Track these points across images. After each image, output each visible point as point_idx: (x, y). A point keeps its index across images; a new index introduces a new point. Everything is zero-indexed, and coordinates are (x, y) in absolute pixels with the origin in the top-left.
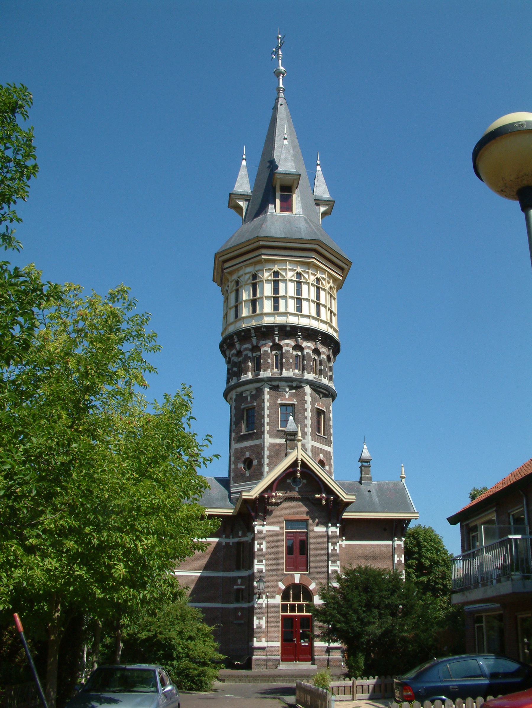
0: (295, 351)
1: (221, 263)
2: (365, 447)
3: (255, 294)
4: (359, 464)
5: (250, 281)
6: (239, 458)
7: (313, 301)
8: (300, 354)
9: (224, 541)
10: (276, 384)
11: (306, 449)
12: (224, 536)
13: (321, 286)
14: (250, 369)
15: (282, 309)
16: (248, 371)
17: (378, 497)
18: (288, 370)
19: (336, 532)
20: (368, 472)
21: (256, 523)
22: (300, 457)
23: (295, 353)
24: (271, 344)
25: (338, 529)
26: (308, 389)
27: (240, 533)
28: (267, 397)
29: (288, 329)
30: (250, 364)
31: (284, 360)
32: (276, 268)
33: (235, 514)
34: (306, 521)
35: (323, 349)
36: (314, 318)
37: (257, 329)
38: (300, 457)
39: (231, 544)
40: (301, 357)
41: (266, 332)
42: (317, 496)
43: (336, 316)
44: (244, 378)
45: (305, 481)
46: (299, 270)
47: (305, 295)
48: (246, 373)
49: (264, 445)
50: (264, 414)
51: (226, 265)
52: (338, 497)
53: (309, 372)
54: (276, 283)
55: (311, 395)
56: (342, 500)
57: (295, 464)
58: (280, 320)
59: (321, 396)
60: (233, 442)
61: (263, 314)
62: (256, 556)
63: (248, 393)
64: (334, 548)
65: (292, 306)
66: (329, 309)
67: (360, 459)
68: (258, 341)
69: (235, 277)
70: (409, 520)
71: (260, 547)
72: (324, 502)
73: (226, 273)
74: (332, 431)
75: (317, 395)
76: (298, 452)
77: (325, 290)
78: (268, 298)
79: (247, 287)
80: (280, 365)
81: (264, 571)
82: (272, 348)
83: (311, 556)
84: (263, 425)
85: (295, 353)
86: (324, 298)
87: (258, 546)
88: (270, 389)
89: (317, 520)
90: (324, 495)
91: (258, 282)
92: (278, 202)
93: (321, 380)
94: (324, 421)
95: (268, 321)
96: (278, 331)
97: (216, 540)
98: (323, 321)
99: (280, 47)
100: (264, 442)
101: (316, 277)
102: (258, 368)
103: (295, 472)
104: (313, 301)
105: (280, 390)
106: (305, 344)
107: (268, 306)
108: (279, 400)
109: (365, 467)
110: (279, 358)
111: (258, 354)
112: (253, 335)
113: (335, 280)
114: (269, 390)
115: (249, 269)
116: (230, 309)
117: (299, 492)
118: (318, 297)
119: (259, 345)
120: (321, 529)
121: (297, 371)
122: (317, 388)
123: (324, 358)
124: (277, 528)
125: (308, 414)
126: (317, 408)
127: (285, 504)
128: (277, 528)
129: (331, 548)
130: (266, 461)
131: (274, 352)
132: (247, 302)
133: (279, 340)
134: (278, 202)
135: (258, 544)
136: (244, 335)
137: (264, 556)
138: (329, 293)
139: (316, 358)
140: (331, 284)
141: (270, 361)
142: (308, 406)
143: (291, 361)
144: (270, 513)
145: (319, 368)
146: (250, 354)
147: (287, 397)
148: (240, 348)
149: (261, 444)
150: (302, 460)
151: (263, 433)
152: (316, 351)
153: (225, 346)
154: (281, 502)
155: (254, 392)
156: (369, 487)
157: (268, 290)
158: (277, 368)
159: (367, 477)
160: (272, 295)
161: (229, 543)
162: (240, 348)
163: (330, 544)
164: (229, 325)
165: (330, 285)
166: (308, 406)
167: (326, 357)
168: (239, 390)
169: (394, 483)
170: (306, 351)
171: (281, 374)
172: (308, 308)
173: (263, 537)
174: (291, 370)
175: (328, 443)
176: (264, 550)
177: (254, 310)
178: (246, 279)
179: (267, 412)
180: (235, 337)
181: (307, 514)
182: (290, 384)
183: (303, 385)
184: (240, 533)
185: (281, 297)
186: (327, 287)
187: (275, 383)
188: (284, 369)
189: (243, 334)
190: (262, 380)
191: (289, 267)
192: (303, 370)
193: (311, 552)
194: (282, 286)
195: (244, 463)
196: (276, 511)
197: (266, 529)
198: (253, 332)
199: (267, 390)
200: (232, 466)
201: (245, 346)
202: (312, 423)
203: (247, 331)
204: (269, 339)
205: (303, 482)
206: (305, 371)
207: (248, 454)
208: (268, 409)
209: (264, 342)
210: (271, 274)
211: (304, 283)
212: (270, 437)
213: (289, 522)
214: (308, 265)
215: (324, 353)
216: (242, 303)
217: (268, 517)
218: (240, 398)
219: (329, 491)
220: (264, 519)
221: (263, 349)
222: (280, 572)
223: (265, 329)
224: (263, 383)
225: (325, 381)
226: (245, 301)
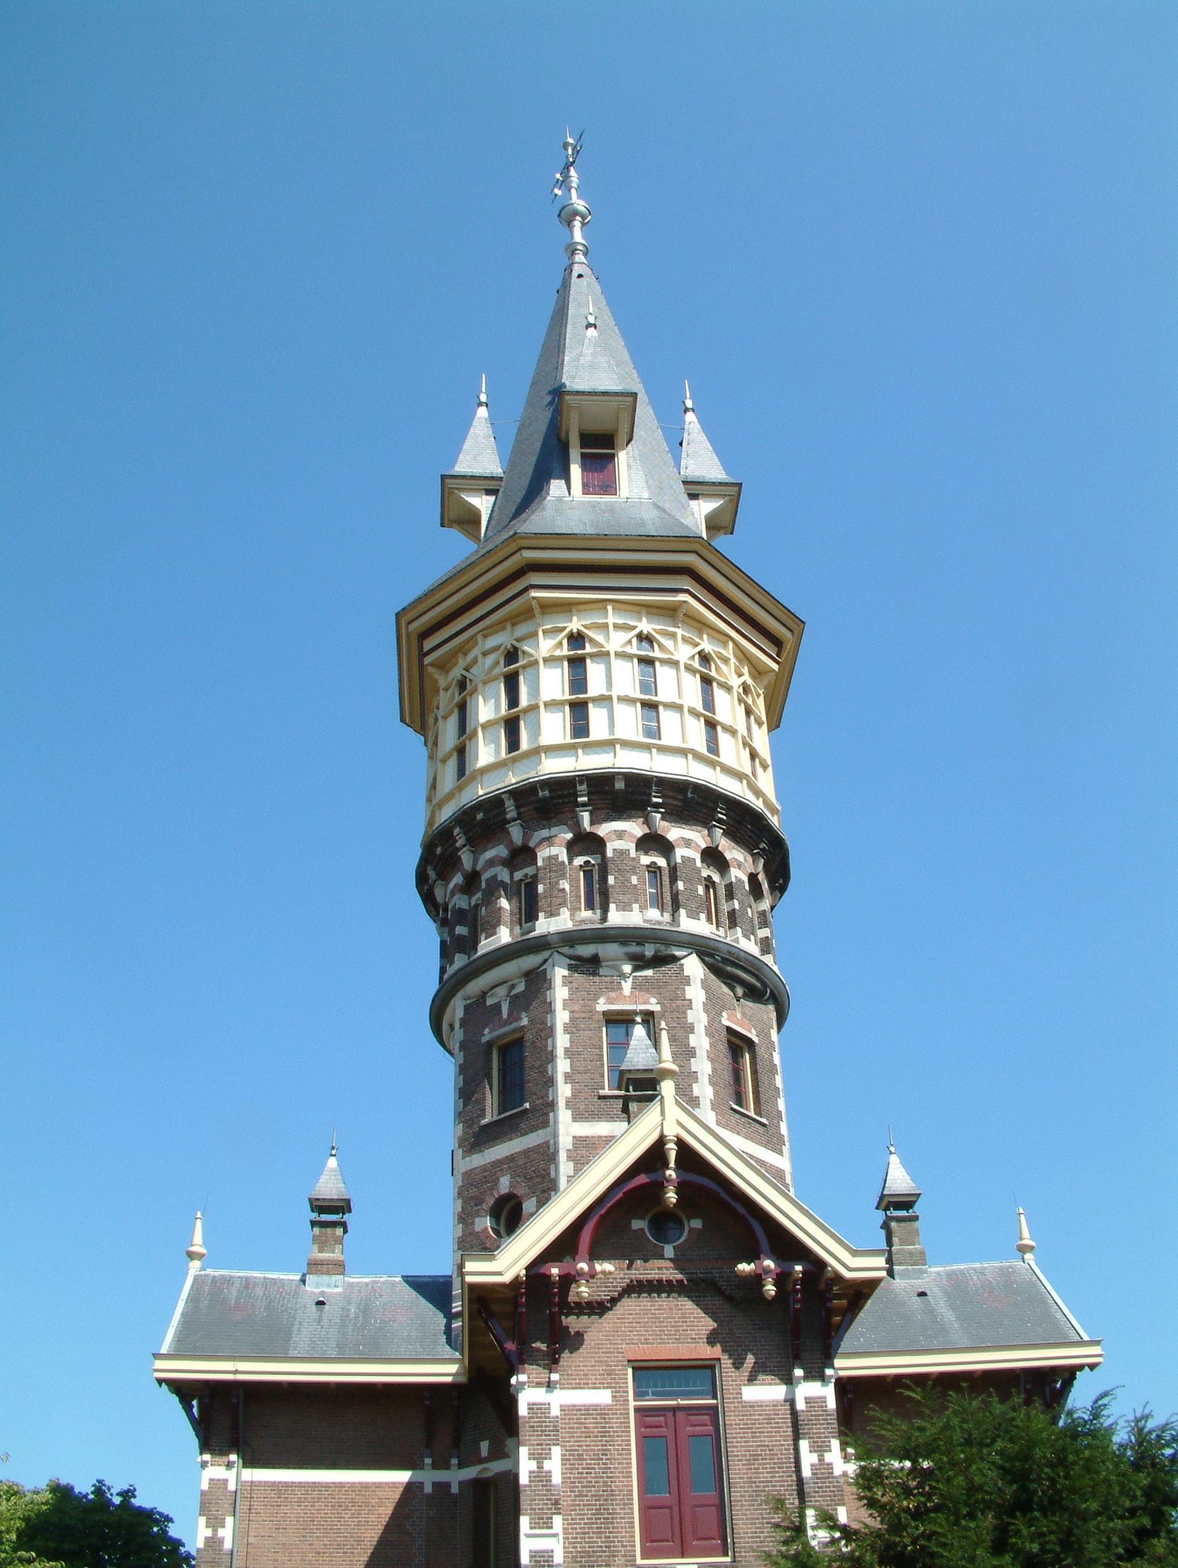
0: (646, 853)
1: (415, 643)
2: (894, 1160)
3: (513, 700)
4: (880, 1216)
5: (502, 669)
6: (479, 1201)
7: (693, 712)
8: (662, 862)
9: (429, 1477)
10: (587, 954)
11: (695, 1102)
12: (428, 1461)
13: (713, 673)
14: (506, 917)
16: (498, 923)
17: (953, 1307)
18: (625, 907)
19: (823, 1399)
20: (911, 1238)
21: (523, 1378)
23: (646, 860)
24: (569, 836)
25: (831, 1387)
26: (693, 966)
27: (484, 1447)
28: (560, 993)
29: (620, 785)
30: (504, 903)
31: (611, 880)
33: (463, 1379)
34: (709, 1367)
35: (733, 852)
36: (697, 756)
37: (524, 794)
38: (671, 1131)
39: (455, 1489)
40: (666, 873)
41: (550, 801)
42: (744, 1267)
43: (770, 770)
44: (486, 945)
45: (697, 1224)
46: (645, 626)
48: (492, 931)
49: (556, 1144)
50: (554, 1046)
51: (428, 644)
52: (821, 1264)
53: (693, 915)
54: (577, 664)
55: (705, 984)
56: (838, 1278)
57: (654, 1157)
59: (740, 991)
61: (537, 752)
62: (524, 1504)
63: (502, 991)
64: (821, 1459)
65: (629, 722)
66: (745, 744)
67: (882, 1197)
68: (528, 829)
69: (456, 672)
70: (1068, 1374)
71: (540, 1467)
72: (770, 1289)
73: (432, 664)
74: (777, 1059)
75: (725, 989)
76: (663, 1113)
77: (729, 689)
78: (552, 705)
79: (491, 687)
80: (599, 894)
81: (558, 1558)
83: (736, 1496)
84: (551, 1082)
86: (727, 709)
87: (533, 1465)
88: (571, 968)
89: (750, 1360)
90: (769, 1263)
91: (524, 667)
92: (576, 471)
93: (737, 940)
94: (755, 1072)
95: (554, 767)
96: (589, 794)
97: (403, 1476)
99: (572, 164)
100: (555, 1135)
101: (698, 649)
103: (659, 1187)
104: (693, 712)
105: (602, 971)
106: (674, 833)
107: (554, 727)
108: (602, 1000)
109: (900, 1220)
110: (596, 877)
111: (530, 871)
112: (511, 813)
113: (758, 672)
114: (566, 972)
116: (444, 761)
117: (677, 1262)
118: (709, 703)
119: (531, 844)
120: (769, 1392)
122: (724, 965)
123: (739, 880)
124: (602, 1397)
125: (700, 1041)
126: (729, 1030)
127: (629, 1305)
128: (602, 1397)
129: (808, 1459)
131: (579, 861)
132: (491, 730)
133: (592, 823)
134: (576, 471)
135: (532, 1456)
136: (484, 821)
137: (556, 1502)
138: (740, 700)
139: (716, 878)
140: (747, 678)
141: (567, 887)
142: (698, 1016)
143: (634, 880)
144: (575, 1341)
145: (725, 907)
146: (504, 875)
147: (628, 991)
148: (475, 862)
149: (547, 1143)
150: (680, 1142)
151: (552, 1106)
152: (713, 856)
153: (432, 874)
154: (614, 1301)
155: (521, 988)
156: (920, 1284)
157: (553, 683)
158: (590, 905)
159: (911, 1253)
160: (567, 696)
161: (447, 1485)
162: (475, 862)
163: (804, 1445)
164: (440, 805)
165: (742, 679)
166: (698, 1016)
167: (746, 879)
168: (474, 987)
169: (1001, 1268)
170: (680, 853)
171: (604, 919)
173: (550, 1429)
174: (636, 906)
175: (774, 1143)
176: (557, 1479)
177: (513, 744)
178: (487, 666)
179: (562, 1041)
180: (457, 831)
181: (712, 1339)
182: (634, 949)
183: (678, 953)
184: (484, 1447)
185: (595, 700)
186: (735, 682)
187: (586, 951)
188: (612, 906)
189: (480, 816)
190: (542, 944)
191: (612, 618)
192: (676, 906)
193: (735, 1478)
194: (595, 671)
195: (495, 1213)
196: (596, 1332)
197: (559, 1400)
198: (510, 805)
199: (560, 973)
201: (489, 854)
202: (714, 1069)
203: (494, 804)
204: (561, 823)
205: (683, 1216)
206: (683, 912)
207: (505, 1184)
208: (566, 1029)
209: (545, 833)
210: (560, 643)
211: (663, 662)
212: (578, 1117)
213: (646, 1371)
214: (670, 613)
215: (739, 866)
216: (475, 733)
217: (566, 1355)
218: (479, 1011)
219: (787, 1246)
220: (552, 1361)
221: (543, 854)
222: (620, 1560)
223: (547, 793)
224: (546, 954)
225: (750, 946)
226: (485, 727)
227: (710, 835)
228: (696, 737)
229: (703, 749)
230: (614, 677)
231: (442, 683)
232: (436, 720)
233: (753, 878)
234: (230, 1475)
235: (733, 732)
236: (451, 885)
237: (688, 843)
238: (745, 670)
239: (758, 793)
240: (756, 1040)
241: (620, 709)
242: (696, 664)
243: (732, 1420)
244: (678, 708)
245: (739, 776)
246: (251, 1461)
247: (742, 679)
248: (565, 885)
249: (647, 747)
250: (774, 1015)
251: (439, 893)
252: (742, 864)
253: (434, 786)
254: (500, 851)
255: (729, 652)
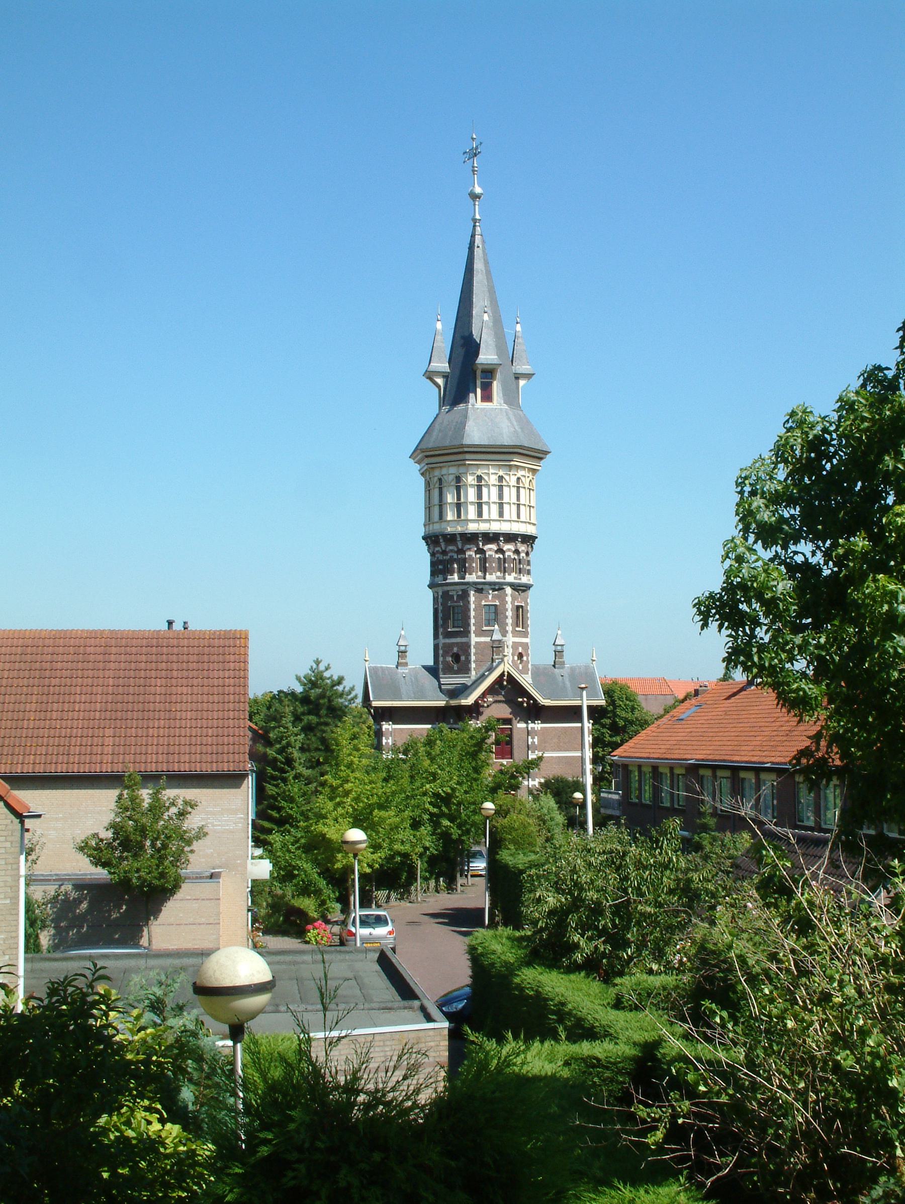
3: (459, 498)
4: (553, 648)
5: (453, 483)
8: (501, 556)
10: (480, 589)
15: (485, 516)
17: (570, 681)
20: (562, 657)
22: (506, 670)
23: (497, 556)
26: (509, 590)
32: (479, 473)
41: (471, 538)
42: (520, 700)
46: (501, 473)
47: (506, 499)
54: (479, 488)
57: (502, 674)
58: (483, 527)
60: (441, 637)
61: (467, 520)
65: (495, 515)
68: (464, 544)
78: (472, 503)
80: (484, 570)
82: (476, 553)
85: (497, 556)
92: (479, 391)
95: (473, 527)
97: (429, 726)
100: (470, 640)
102: (463, 571)
106: (506, 547)
115: (453, 470)
120: (522, 725)
121: (498, 574)
125: (509, 613)
129: (530, 740)
130: (473, 658)
131: (478, 556)
134: (479, 391)
136: (451, 538)
142: (509, 606)
147: (491, 598)
151: (469, 632)
157: (472, 495)
166: (509, 606)
170: (507, 554)
172: (510, 512)
177: (459, 516)
179: (472, 613)
187: (480, 587)
190: (468, 583)
191: (492, 471)
192: (505, 572)
194: (485, 490)
199: (472, 593)
200: (441, 659)
201: (451, 548)
205: (508, 688)
207: (455, 650)
209: (468, 546)
218: (446, 595)
219: (530, 697)
221: (468, 553)
229: (515, 517)
230: (491, 494)
234: (390, 727)
241: (492, 506)
243: (515, 731)
244: (509, 504)
246: (394, 724)
248: (474, 565)
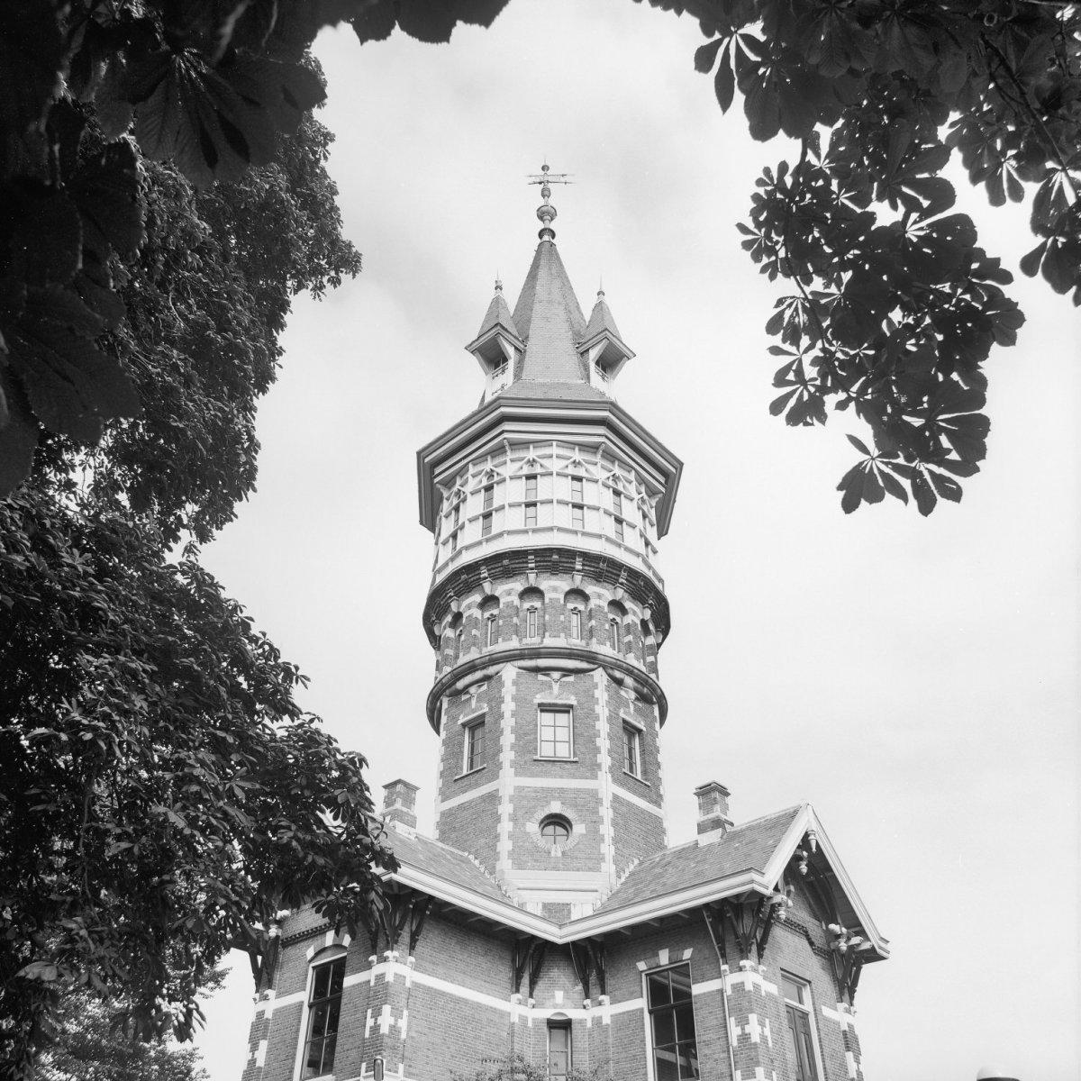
7: (606, 512)
8: (581, 607)
13: (620, 488)
26: (600, 676)
28: (508, 691)
36: (608, 539)
51: (437, 471)
66: (642, 536)
86: (630, 512)
98: (627, 549)
101: (612, 473)
104: (606, 512)
106: (590, 589)
113: (652, 492)
116: (444, 543)
125: (603, 727)
126: (625, 721)
142: (602, 710)
148: (459, 607)
151: (499, 766)
152: (617, 605)
165: (641, 496)
166: (602, 710)
167: (639, 623)
170: (593, 603)
177: (487, 528)
186: (637, 497)
203: (472, 568)
227: (614, 593)
228: (609, 527)
231: (445, 494)
232: (440, 519)
233: (644, 623)
235: (634, 527)
236: (443, 625)
237: (599, 596)
238: (643, 489)
239: (650, 567)
240: (644, 729)
242: (610, 483)
245: (638, 555)
247: (641, 496)
249: (576, 532)
250: (656, 713)
251: (437, 630)
252: (637, 613)
253: (436, 561)
254: (477, 598)
255: (632, 476)
